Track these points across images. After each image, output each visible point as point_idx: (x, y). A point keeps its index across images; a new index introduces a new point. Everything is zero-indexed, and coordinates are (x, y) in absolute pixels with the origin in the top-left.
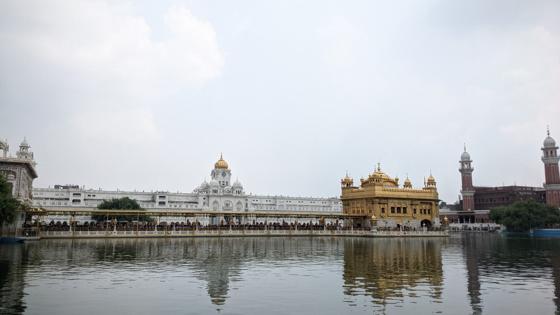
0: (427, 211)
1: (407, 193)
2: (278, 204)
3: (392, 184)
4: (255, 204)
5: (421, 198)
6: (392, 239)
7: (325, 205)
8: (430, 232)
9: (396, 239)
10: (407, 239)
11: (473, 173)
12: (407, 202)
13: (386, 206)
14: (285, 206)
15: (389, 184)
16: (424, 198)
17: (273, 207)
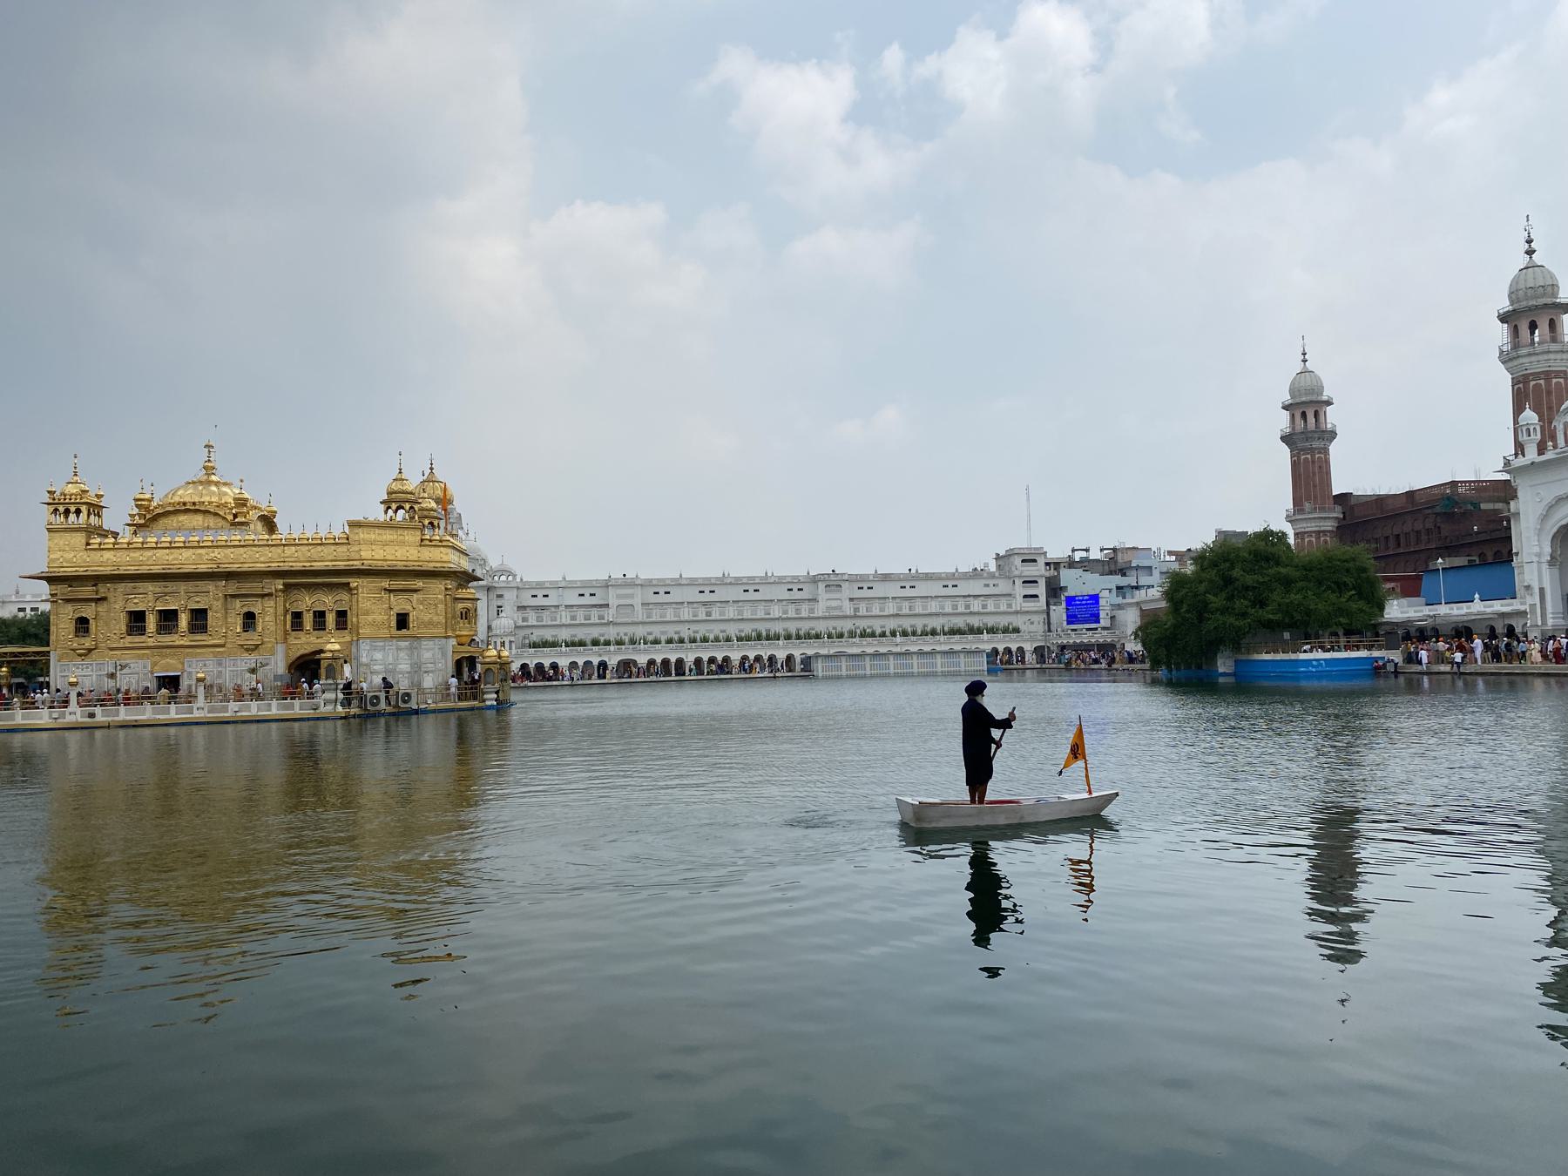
0: (331, 619)
1: (216, 553)
2: (613, 602)
3: (211, 521)
4: (543, 608)
5: (285, 567)
6: (18, 739)
7: (799, 595)
8: (233, 705)
9: (45, 735)
10: (98, 733)
11: (1334, 448)
12: (210, 586)
13: (102, 608)
14: (639, 608)
15: (198, 520)
16: (298, 566)
17: (595, 613)
